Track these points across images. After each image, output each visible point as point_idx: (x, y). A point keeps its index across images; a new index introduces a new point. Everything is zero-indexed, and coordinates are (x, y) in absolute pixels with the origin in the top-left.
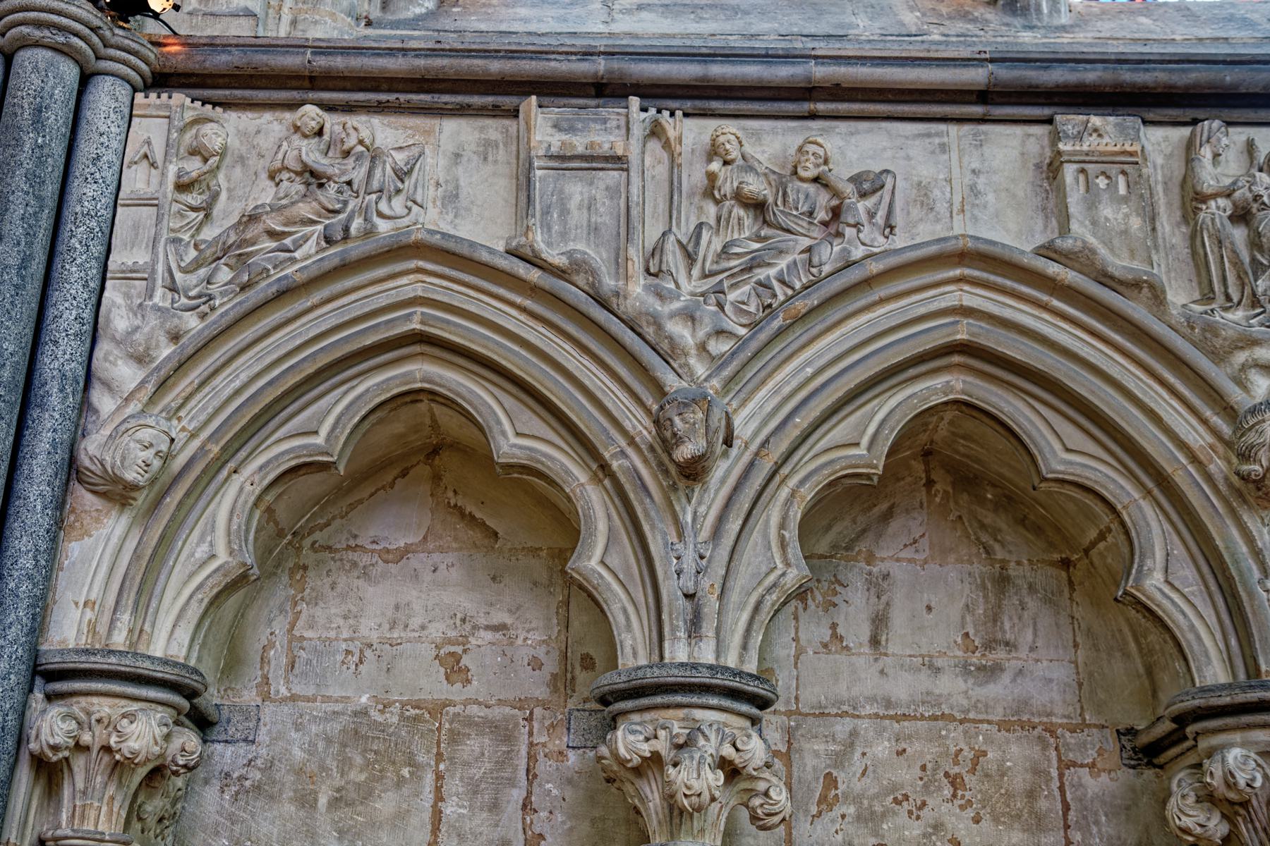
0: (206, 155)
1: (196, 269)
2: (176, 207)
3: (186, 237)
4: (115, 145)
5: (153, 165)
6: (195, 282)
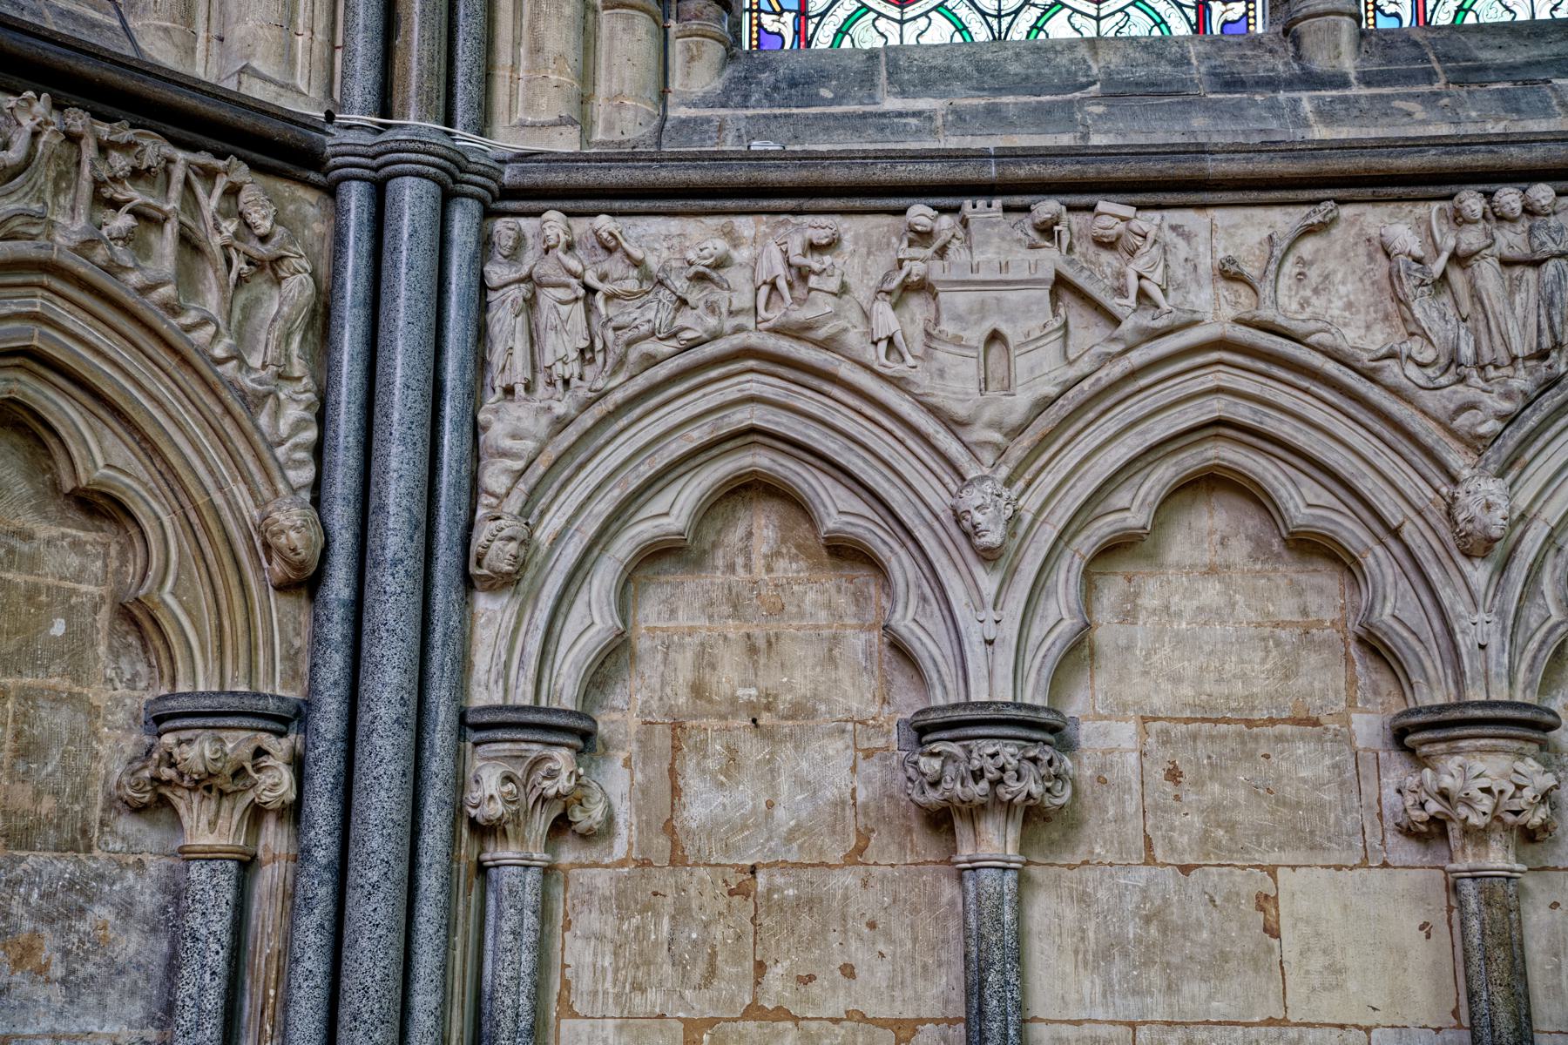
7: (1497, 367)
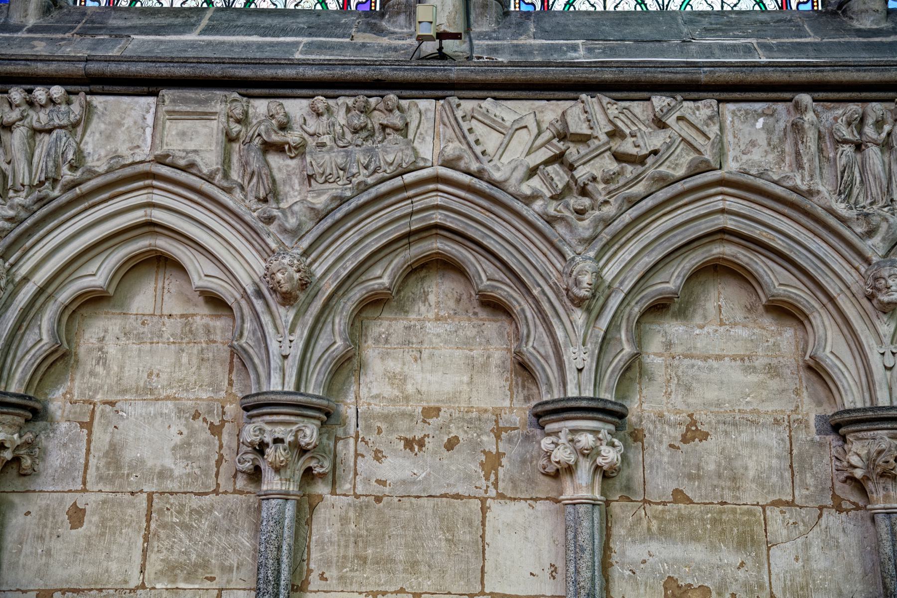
7: (16, 191)
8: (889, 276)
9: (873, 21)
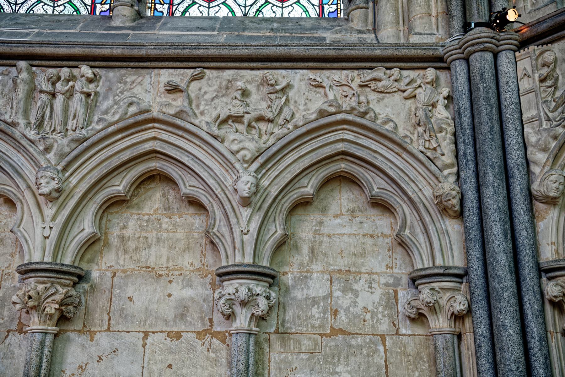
0: (548, 65)
1: (556, 110)
2: (542, 89)
3: (549, 99)
4: (512, 75)
5: (529, 77)
6: (557, 114)
8: (41, 177)
9: (121, 22)
